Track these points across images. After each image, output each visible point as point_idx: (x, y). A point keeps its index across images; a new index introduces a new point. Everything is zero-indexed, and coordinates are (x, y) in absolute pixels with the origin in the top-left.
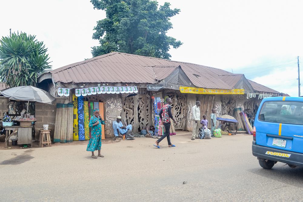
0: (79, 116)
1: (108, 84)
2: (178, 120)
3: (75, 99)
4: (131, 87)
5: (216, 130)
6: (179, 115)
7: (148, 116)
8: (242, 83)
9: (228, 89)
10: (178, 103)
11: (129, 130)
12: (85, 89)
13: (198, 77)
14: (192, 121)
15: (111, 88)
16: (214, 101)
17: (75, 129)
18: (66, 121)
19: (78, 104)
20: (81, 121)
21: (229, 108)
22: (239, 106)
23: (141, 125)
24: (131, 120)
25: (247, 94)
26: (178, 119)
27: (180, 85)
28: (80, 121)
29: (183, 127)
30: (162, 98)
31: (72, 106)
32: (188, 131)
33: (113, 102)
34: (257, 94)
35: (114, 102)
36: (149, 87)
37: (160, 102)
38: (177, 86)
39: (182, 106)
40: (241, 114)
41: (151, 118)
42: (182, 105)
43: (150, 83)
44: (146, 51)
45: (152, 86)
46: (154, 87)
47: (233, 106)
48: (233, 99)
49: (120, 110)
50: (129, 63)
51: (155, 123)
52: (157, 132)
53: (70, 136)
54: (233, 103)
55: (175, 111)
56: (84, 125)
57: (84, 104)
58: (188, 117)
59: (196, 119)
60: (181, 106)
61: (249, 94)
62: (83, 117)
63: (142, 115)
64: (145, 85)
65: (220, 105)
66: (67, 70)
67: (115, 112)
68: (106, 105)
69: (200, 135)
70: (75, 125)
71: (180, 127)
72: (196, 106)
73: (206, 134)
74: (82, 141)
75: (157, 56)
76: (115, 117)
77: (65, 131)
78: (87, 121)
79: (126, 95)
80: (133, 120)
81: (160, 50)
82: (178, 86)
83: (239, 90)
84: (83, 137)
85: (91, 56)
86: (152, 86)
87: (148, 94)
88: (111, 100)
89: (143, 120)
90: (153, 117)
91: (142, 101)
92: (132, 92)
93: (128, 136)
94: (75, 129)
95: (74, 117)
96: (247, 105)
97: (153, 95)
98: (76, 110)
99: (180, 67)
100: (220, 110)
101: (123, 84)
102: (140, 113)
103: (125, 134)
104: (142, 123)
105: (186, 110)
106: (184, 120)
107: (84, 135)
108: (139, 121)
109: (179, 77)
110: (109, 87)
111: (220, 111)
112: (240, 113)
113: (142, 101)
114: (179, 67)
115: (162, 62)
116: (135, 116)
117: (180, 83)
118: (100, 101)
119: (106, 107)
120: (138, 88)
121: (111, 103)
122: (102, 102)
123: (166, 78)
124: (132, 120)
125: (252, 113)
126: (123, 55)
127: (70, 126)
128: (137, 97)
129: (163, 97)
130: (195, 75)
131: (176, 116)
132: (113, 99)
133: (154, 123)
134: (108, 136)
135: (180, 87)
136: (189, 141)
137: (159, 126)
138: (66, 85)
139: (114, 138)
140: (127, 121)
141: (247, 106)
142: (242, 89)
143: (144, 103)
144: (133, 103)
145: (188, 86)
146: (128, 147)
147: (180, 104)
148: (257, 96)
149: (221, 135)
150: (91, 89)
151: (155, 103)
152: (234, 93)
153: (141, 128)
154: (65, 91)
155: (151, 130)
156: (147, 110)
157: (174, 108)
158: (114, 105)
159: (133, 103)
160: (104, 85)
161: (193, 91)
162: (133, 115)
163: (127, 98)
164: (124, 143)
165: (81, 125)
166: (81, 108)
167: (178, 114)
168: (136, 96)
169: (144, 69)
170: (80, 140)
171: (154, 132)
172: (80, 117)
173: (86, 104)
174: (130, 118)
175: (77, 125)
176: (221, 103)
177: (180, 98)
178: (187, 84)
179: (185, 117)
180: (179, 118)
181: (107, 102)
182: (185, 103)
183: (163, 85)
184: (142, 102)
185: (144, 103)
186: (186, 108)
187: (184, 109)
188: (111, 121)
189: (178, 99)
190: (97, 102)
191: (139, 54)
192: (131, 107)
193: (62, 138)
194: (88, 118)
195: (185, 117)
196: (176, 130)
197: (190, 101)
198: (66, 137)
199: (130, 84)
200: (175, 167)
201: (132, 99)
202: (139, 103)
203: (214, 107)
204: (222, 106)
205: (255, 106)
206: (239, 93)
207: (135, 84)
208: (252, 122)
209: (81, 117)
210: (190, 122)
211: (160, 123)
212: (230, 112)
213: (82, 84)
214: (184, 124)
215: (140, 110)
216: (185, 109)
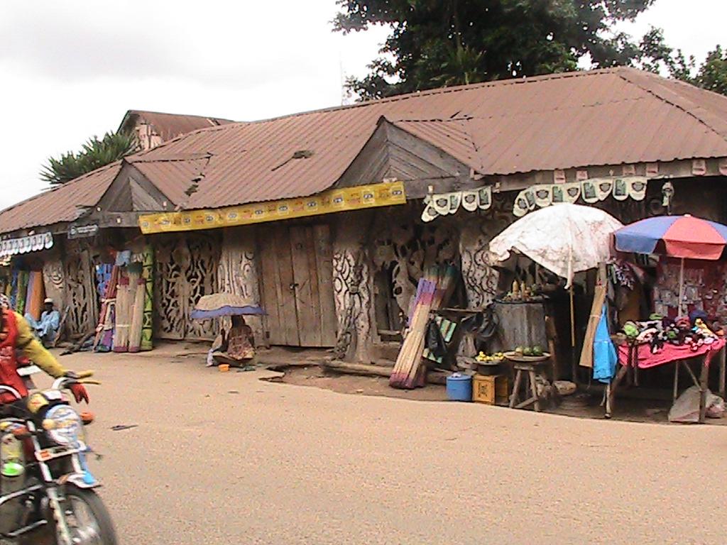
10: (192, 260)
54: (438, 240)
60: (203, 271)
65: (350, 257)
80: (84, 309)
110: (12, 240)
120: (53, 235)
145: (160, 212)
162: (84, 297)
167: (197, 295)
174: (80, 305)
178: (156, 206)
183: (98, 220)
189: (190, 251)
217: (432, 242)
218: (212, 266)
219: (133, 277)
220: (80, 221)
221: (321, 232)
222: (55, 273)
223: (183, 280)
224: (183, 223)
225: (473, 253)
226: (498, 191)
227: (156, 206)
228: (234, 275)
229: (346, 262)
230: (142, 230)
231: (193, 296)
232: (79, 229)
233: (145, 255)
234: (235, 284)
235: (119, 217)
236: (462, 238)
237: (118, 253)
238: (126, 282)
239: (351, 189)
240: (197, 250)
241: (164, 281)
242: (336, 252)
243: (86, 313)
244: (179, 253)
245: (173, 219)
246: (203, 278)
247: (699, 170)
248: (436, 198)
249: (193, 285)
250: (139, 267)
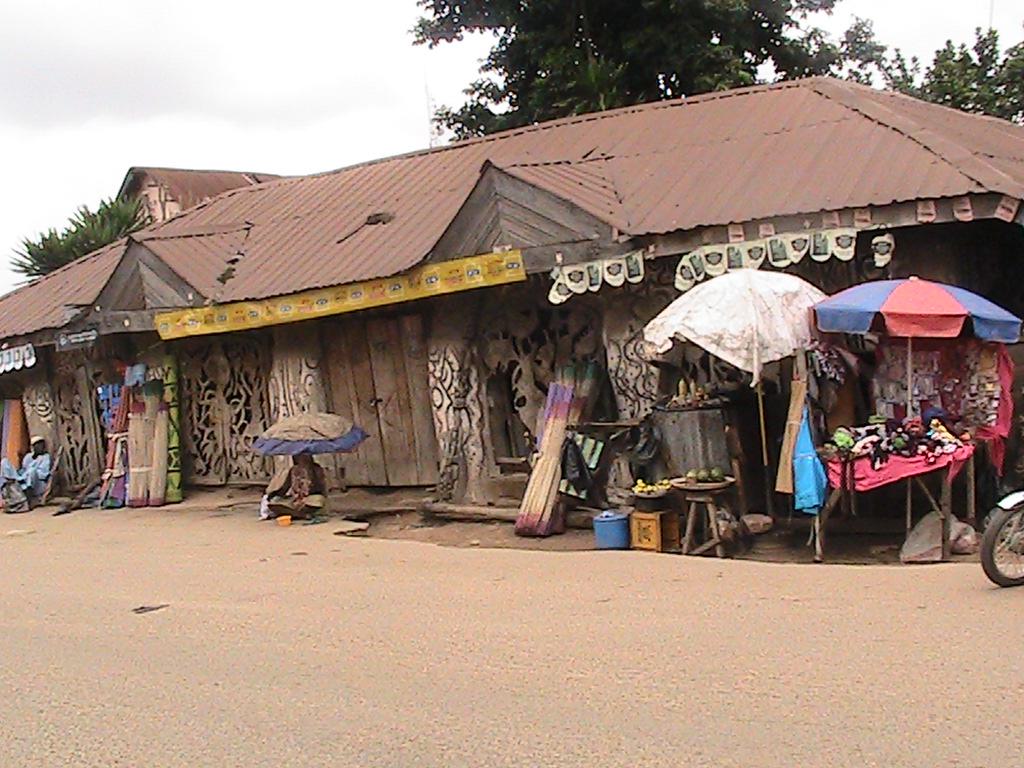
6: (244, 426)
10: (232, 372)
27: (156, 311)
36: (62, 340)
39: (251, 388)
55: (226, 407)
65: (452, 358)
80: (84, 450)
120: (35, 349)
131: (233, 432)
135: (156, 317)
145: (184, 308)
157: (219, 394)
162: (83, 433)
167: (241, 421)
174: (77, 444)
177: (239, 354)
178: (179, 300)
183: (98, 324)
189: (228, 359)
197: (290, 362)
217: (564, 331)
218: (260, 382)
219: (150, 401)
220: (71, 327)
221: (411, 325)
222: (40, 401)
225: (622, 344)
226: (651, 256)
227: (179, 300)
228: (292, 391)
229: (447, 366)
230: (161, 334)
231: (236, 424)
232: (70, 337)
234: (294, 403)
235: (127, 318)
236: (605, 326)
237: (128, 368)
238: (141, 407)
239: (450, 263)
240: (239, 359)
241: (194, 406)
242: (433, 351)
243: (87, 454)
244: (213, 363)
245: (203, 318)
246: (248, 397)
247: (928, 216)
248: (567, 270)
249: (235, 408)
250: (157, 387)
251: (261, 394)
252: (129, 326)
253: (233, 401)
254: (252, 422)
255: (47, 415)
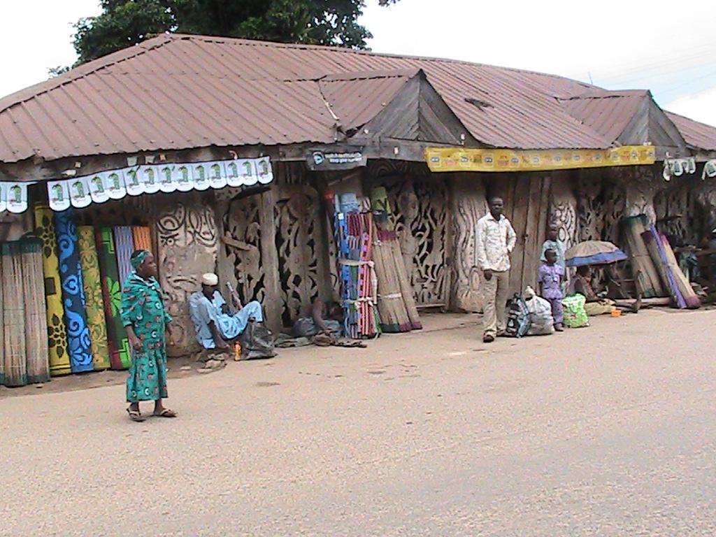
0: (66, 281)
1: (163, 157)
2: (424, 275)
3: (45, 220)
4: (250, 161)
5: (568, 301)
6: (426, 255)
7: (314, 264)
8: (645, 121)
9: (599, 149)
10: (420, 210)
11: (252, 321)
12: (81, 179)
13: (481, 107)
14: (476, 275)
15: (176, 171)
16: (549, 196)
17: (55, 333)
18: (21, 307)
19: (57, 238)
20: (75, 303)
21: (601, 216)
22: (636, 208)
23: (292, 302)
24: (253, 284)
25: (663, 162)
26: (423, 269)
28: (69, 302)
29: (442, 297)
30: (360, 194)
31: (38, 246)
32: (466, 312)
33: (184, 221)
34: (700, 159)
35: (188, 223)
36: (316, 158)
37: (355, 211)
38: (417, 145)
40: (647, 236)
41: (327, 274)
42: (436, 216)
43: (317, 143)
44: (284, 21)
45: (324, 153)
46: (332, 155)
47: (617, 209)
48: (613, 185)
49: (212, 249)
50: (227, 72)
51: (343, 291)
52: (357, 324)
53: (38, 358)
55: (412, 239)
56: (85, 317)
57: (80, 237)
58: (459, 259)
59: (487, 266)
60: (431, 221)
61: (670, 161)
62: (78, 284)
63: (293, 266)
64: (299, 152)
65: (572, 209)
66: (8, 114)
67: (193, 259)
68: (160, 235)
69: (511, 324)
70: (55, 316)
71: (434, 298)
72: (489, 216)
73: (534, 317)
74: (86, 376)
75: (321, 37)
76: (194, 276)
77: (19, 342)
78: (96, 299)
79: (230, 192)
80: (260, 284)
81: (328, 18)
82: (419, 148)
83: (634, 148)
84: (87, 361)
85: (72, 57)
86: (324, 153)
87: (308, 184)
88: (177, 216)
89: (297, 281)
90: (333, 270)
91: (288, 210)
92: (251, 181)
93: (251, 345)
94: (55, 333)
95: (49, 289)
96: (664, 203)
97: (330, 184)
98: (53, 261)
99: (421, 75)
100: (573, 225)
101: (221, 153)
102: (286, 256)
103: (239, 338)
104: (296, 295)
105: (450, 237)
106: (445, 272)
107: (89, 351)
108: (284, 287)
109: (420, 113)
110: (170, 166)
111: (572, 230)
112: (642, 234)
113: (288, 210)
114: (418, 77)
115: (349, 59)
116: (268, 269)
117: (428, 136)
118: (137, 222)
119: (160, 244)
121: (177, 226)
122: (144, 224)
123: (374, 119)
124: (258, 283)
125: (684, 232)
126: (202, 44)
127: (37, 323)
128: (271, 197)
129: (366, 192)
130: (472, 101)
131: (415, 261)
132: (182, 210)
133: (337, 292)
134: (175, 352)
135: (427, 148)
136: (476, 348)
137: (361, 302)
138: (12, 171)
139: (199, 355)
140: (240, 288)
141: (664, 208)
142: (645, 144)
143: (296, 219)
144: (257, 219)
146: (261, 384)
147: (428, 214)
148: (700, 166)
149: (586, 319)
150: (105, 177)
151: (341, 216)
152: (619, 161)
153: (293, 313)
154: (11, 194)
155: (329, 316)
156: (311, 243)
158: (188, 234)
159: (257, 219)
160: (151, 162)
161: (475, 161)
162: (260, 264)
163: (234, 204)
164: (238, 375)
165: (76, 317)
166: (68, 252)
168: (267, 195)
169: (286, 89)
170: (77, 371)
171: (342, 323)
172: (68, 286)
173: (86, 237)
174: (250, 278)
175: (60, 314)
176: (575, 203)
178: (450, 137)
179: (450, 261)
180: (427, 267)
181: (162, 222)
182: (446, 209)
183: (364, 147)
184: (291, 217)
185: (296, 219)
186: (450, 225)
187: (443, 233)
188: (183, 295)
189: (418, 197)
190: (125, 225)
191: (252, 34)
192: (252, 235)
193: (10, 370)
194: (99, 287)
195: (447, 259)
196: (420, 311)
197: (465, 202)
198: (24, 365)
199: (243, 150)
200: (456, 443)
201: (253, 206)
202: (280, 220)
203: (550, 218)
204: (579, 210)
205: (692, 204)
206: (636, 161)
207: (262, 149)
208: (689, 262)
209: (73, 285)
210: (469, 277)
211: (362, 289)
212: (608, 234)
213: (69, 161)
214: (447, 288)
215: (285, 244)
216: (446, 230)
220: (333, 147)
223: (407, 233)
224: (484, 163)
225: (642, 207)
229: (569, 213)
231: (418, 254)
232: (327, 156)
233: (383, 202)
236: (627, 196)
240: (427, 197)
242: (560, 203)
243: (262, 289)
244: (405, 199)
245: (472, 157)
246: (432, 230)
249: (419, 240)
251: (444, 228)
252: (398, 154)
253: (419, 233)
254: (432, 252)
255: (213, 246)
